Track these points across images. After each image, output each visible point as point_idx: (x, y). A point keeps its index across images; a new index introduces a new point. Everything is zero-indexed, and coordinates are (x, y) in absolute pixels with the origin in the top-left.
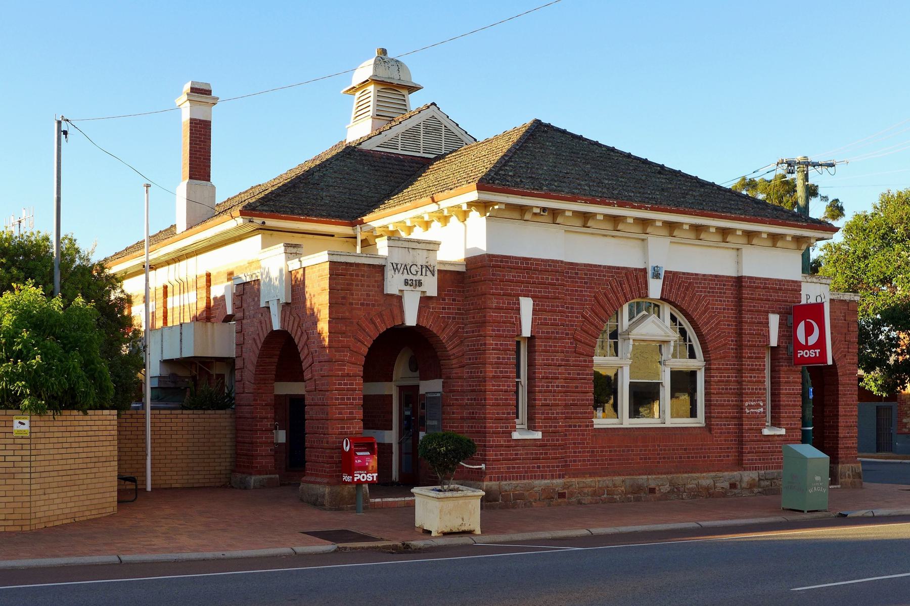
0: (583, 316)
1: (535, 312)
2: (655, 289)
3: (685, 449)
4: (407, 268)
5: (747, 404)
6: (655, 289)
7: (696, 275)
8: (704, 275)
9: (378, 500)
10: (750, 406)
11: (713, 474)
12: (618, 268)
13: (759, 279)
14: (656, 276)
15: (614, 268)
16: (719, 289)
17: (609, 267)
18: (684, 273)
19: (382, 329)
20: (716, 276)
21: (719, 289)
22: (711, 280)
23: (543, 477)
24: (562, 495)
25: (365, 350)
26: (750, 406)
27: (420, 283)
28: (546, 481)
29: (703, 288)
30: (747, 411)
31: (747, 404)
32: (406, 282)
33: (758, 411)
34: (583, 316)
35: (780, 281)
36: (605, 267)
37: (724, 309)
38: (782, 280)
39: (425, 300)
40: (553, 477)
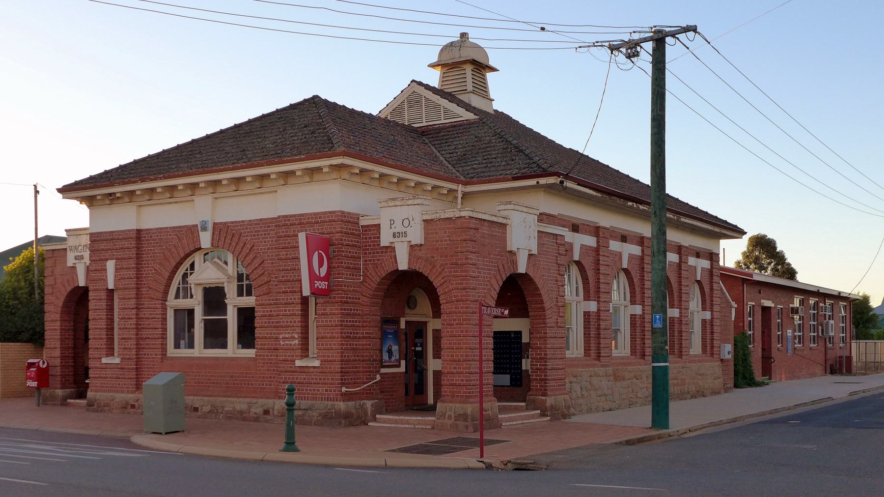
0: (155, 270)
1: (117, 270)
2: (205, 239)
3: (232, 377)
4: (76, 248)
6: (205, 239)
7: (243, 221)
8: (250, 221)
9: (72, 401)
11: (248, 400)
12: (180, 227)
13: (295, 216)
14: (204, 229)
15: (177, 227)
16: (263, 231)
17: (174, 228)
18: (232, 222)
19: (69, 289)
20: (261, 220)
21: (263, 231)
22: (256, 224)
23: (122, 392)
24: (133, 406)
25: (61, 304)
28: (123, 395)
29: (249, 232)
32: (76, 259)
34: (155, 270)
35: (316, 214)
36: (171, 228)
37: (268, 249)
38: (318, 213)
40: (128, 392)
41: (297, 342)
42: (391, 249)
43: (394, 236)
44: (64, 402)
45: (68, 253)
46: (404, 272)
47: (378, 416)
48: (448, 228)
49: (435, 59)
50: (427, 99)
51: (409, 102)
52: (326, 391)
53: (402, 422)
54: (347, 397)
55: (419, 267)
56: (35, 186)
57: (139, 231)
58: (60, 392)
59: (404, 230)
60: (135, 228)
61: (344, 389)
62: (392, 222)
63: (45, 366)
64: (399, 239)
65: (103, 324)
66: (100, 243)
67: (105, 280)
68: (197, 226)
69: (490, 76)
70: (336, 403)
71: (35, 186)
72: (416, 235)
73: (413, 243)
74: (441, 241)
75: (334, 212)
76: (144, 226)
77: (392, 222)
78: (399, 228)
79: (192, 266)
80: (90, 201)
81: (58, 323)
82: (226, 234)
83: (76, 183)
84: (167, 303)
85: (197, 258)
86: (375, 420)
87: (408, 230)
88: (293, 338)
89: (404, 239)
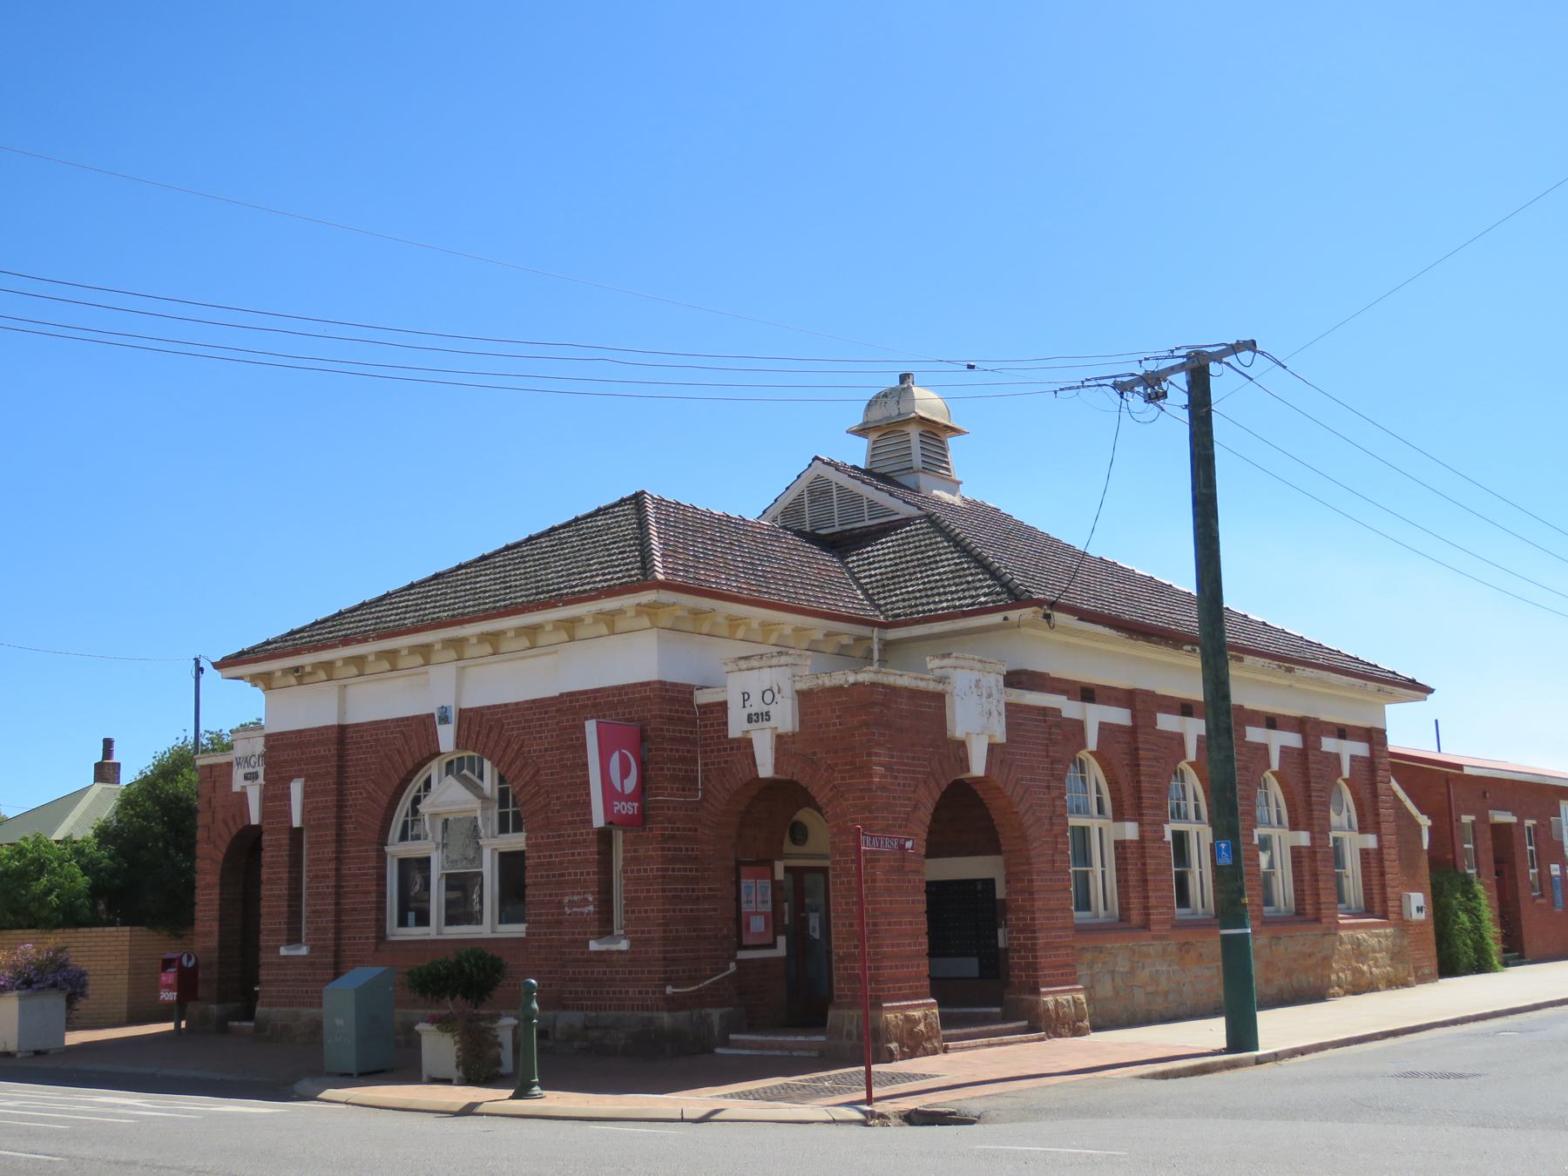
1: (307, 794)
2: (446, 737)
4: (247, 760)
5: (566, 899)
6: (446, 737)
10: (572, 904)
14: (445, 720)
17: (398, 720)
19: (234, 831)
25: (221, 857)
26: (572, 904)
30: (567, 910)
31: (566, 899)
33: (586, 910)
38: (623, 687)
41: (591, 908)
42: (746, 744)
43: (750, 719)
44: (222, 1027)
45: (235, 768)
46: (770, 784)
47: (732, 1037)
48: (838, 703)
49: (858, 420)
50: (840, 488)
51: (811, 492)
53: (771, 1046)
54: (674, 1003)
56: (197, 661)
57: (342, 729)
58: (214, 1009)
59: (765, 709)
60: (335, 722)
61: (669, 990)
62: (746, 696)
63: (191, 964)
65: (282, 889)
66: (285, 752)
67: (288, 815)
68: (432, 715)
69: (952, 442)
70: (656, 1014)
71: (197, 661)
72: (785, 717)
73: (780, 731)
74: (828, 726)
75: (648, 684)
76: (351, 720)
77: (746, 696)
78: (756, 706)
79: (428, 784)
80: (265, 681)
81: (217, 891)
82: (482, 727)
83: (242, 653)
84: (387, 849)
85: (434, 769)
86: (727, 1043)
87: (772, 709)
88: (585, 902)
89: (766, 724)
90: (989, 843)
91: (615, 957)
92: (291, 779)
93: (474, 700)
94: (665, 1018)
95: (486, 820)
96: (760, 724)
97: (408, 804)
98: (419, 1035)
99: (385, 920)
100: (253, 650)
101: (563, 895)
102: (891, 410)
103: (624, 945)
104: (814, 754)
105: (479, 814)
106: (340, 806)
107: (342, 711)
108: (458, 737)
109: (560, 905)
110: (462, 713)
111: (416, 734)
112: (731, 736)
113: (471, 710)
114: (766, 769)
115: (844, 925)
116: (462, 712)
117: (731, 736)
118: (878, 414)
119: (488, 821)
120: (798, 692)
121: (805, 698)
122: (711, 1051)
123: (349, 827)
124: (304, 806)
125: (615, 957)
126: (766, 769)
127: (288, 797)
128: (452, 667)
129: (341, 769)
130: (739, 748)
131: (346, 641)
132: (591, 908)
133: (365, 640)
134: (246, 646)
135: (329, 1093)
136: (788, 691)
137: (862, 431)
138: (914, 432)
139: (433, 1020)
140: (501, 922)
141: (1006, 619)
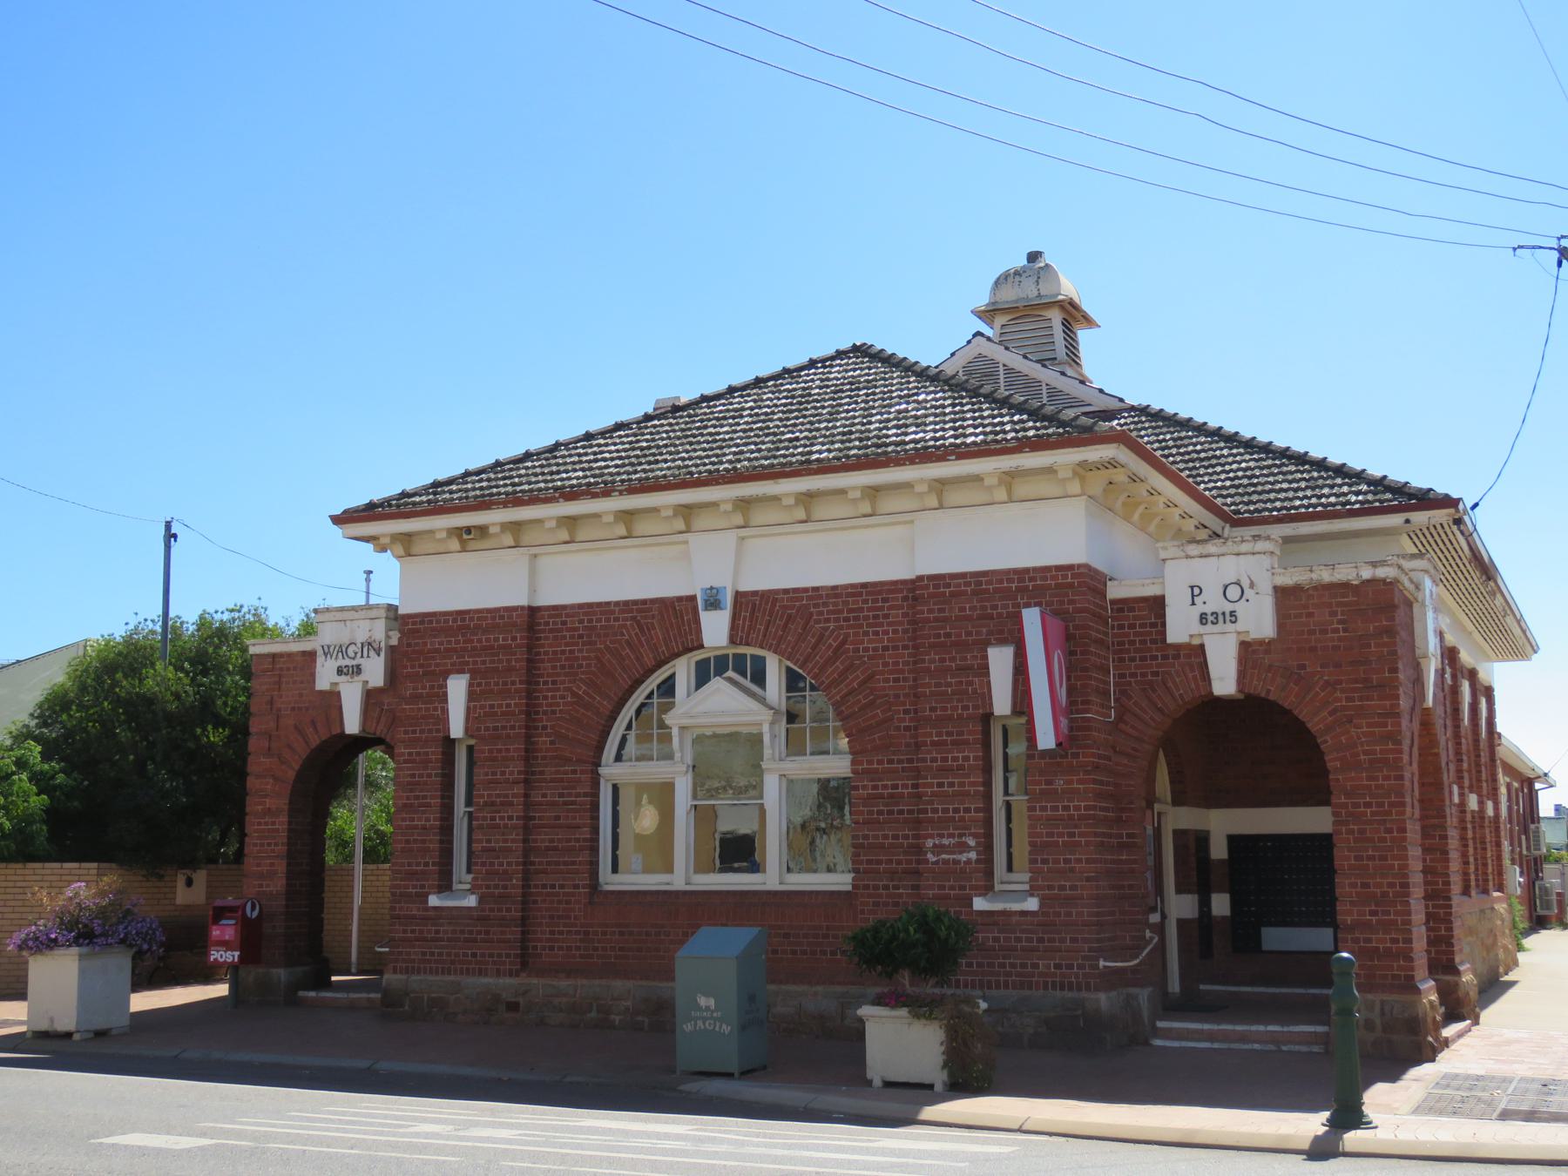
0: (574, 694)
1: (472, 696)
2: (715, 629)
3: (787, 936)
4: (342, 650)
5: (930, 843)
6: (715, 629)
7: (816, 589)
8: (835, 588)
9: (312, 994)
10: (939, 849)
11: (839, 989)
12: (644, 602)
13: (963, 575)
14: (713, 603)
15: (635, 602)
16: (869, 609)
17: (626, 603)
18: (786, 591)
19: (315, 741)
20: (864, 585)
21: (869, 609)
22: (853, 595)
23: (481, 973)
24: (513, 1007)
25: (291, 775)
26: (939, 849)
27: (358, 670)
28: (485, 980)
29: (833, 612)
30: (931, 857)
31: (930, 843)
32: (340, 671)
33: (964, 857)
34: (574, 694)
35: (1021, 573)
36: (617, 603)
37: (885, 648)
38: (1026, 570)
39: (370, 696)
40: (498, 973)
41: (973, 855)
43: (1203, 618)
45: (320, 660)
46: (1219, 699)
47: (1160, 1024)
48: (1339, 604)
49: (983, 300)
50: (1009, 370)
52: (474, 955)
53: (1243, 1038)
54: (1113, 980)
55: (1258, 688)
56: (168, 525)
57: (533, 611)
58: (281, 974)
59: (1228, 607)
60: (524, 602)
62: (1195, 591)
63: (255, 914)
64: (1216, 628)
66: (421, 644)
68: (693, 598)
69: (1083, 336)
70: (1084, 994)
71: (168, 525)
72: (1260, 620)
74: (1325, 631)
75: (1070, 567)
76: (546, 599)
77: (1195, 591)
78: (1213, 602)
79: (668, 688)
80: (406, 545)
81: (284, 818)
82: (760, 614)
83: (371, 506)
84: (602, 770)
85: (683, 669)
86: (1157, 1033)
87: (1240, 608)
88: (963, 847)
89: (1230, 627)
90: (1312, 786)
91: (1015, 919)
92: (446, 675)
93: (756, 581)
94: (1104, 1000)
95: (773, 736)
96: (1220, 627)
97: (632, 712)
98: (861, 1021)
99: (597, 863)
100: (386, 502)
101: (927, 837)
102: (1028, 290)
103: (471, 901)
104: (1303, 667)
105: (766, 728)
106: (530, 711)
107: (533, 590)
108: (734, 627)
109: (919, 850)
110: (739, 596)
111: (672, 622)
112: (1170, 640)
113: (755, 593)
114: (1224, 682)
115: (1353, 885)
116: (739, 596)
117: (1170, 640)
118: (1009, 295)
119: (773, 737)
120: (1276, 589)
121: (1283, 594)
122: (1146, 1043)
123: (543, 740)
124: (469, 711)
125: (1015, 919)
126: (1224, 682)
127: (984, 670)
128: (732, 536)
129: (532, 663)
130: (1177, 657)
131: (515, 501)
132: (973, 855)
133: (606, 493)
134: (377, 496)
135: (929, 1113)
136: (1265, 586)
137: (987, 314)
138: (1056, 317)
139: (879, 1001)
140: (696, 872)
141: (1407, 521)
